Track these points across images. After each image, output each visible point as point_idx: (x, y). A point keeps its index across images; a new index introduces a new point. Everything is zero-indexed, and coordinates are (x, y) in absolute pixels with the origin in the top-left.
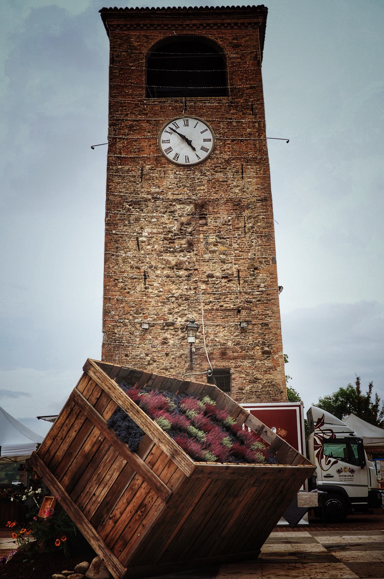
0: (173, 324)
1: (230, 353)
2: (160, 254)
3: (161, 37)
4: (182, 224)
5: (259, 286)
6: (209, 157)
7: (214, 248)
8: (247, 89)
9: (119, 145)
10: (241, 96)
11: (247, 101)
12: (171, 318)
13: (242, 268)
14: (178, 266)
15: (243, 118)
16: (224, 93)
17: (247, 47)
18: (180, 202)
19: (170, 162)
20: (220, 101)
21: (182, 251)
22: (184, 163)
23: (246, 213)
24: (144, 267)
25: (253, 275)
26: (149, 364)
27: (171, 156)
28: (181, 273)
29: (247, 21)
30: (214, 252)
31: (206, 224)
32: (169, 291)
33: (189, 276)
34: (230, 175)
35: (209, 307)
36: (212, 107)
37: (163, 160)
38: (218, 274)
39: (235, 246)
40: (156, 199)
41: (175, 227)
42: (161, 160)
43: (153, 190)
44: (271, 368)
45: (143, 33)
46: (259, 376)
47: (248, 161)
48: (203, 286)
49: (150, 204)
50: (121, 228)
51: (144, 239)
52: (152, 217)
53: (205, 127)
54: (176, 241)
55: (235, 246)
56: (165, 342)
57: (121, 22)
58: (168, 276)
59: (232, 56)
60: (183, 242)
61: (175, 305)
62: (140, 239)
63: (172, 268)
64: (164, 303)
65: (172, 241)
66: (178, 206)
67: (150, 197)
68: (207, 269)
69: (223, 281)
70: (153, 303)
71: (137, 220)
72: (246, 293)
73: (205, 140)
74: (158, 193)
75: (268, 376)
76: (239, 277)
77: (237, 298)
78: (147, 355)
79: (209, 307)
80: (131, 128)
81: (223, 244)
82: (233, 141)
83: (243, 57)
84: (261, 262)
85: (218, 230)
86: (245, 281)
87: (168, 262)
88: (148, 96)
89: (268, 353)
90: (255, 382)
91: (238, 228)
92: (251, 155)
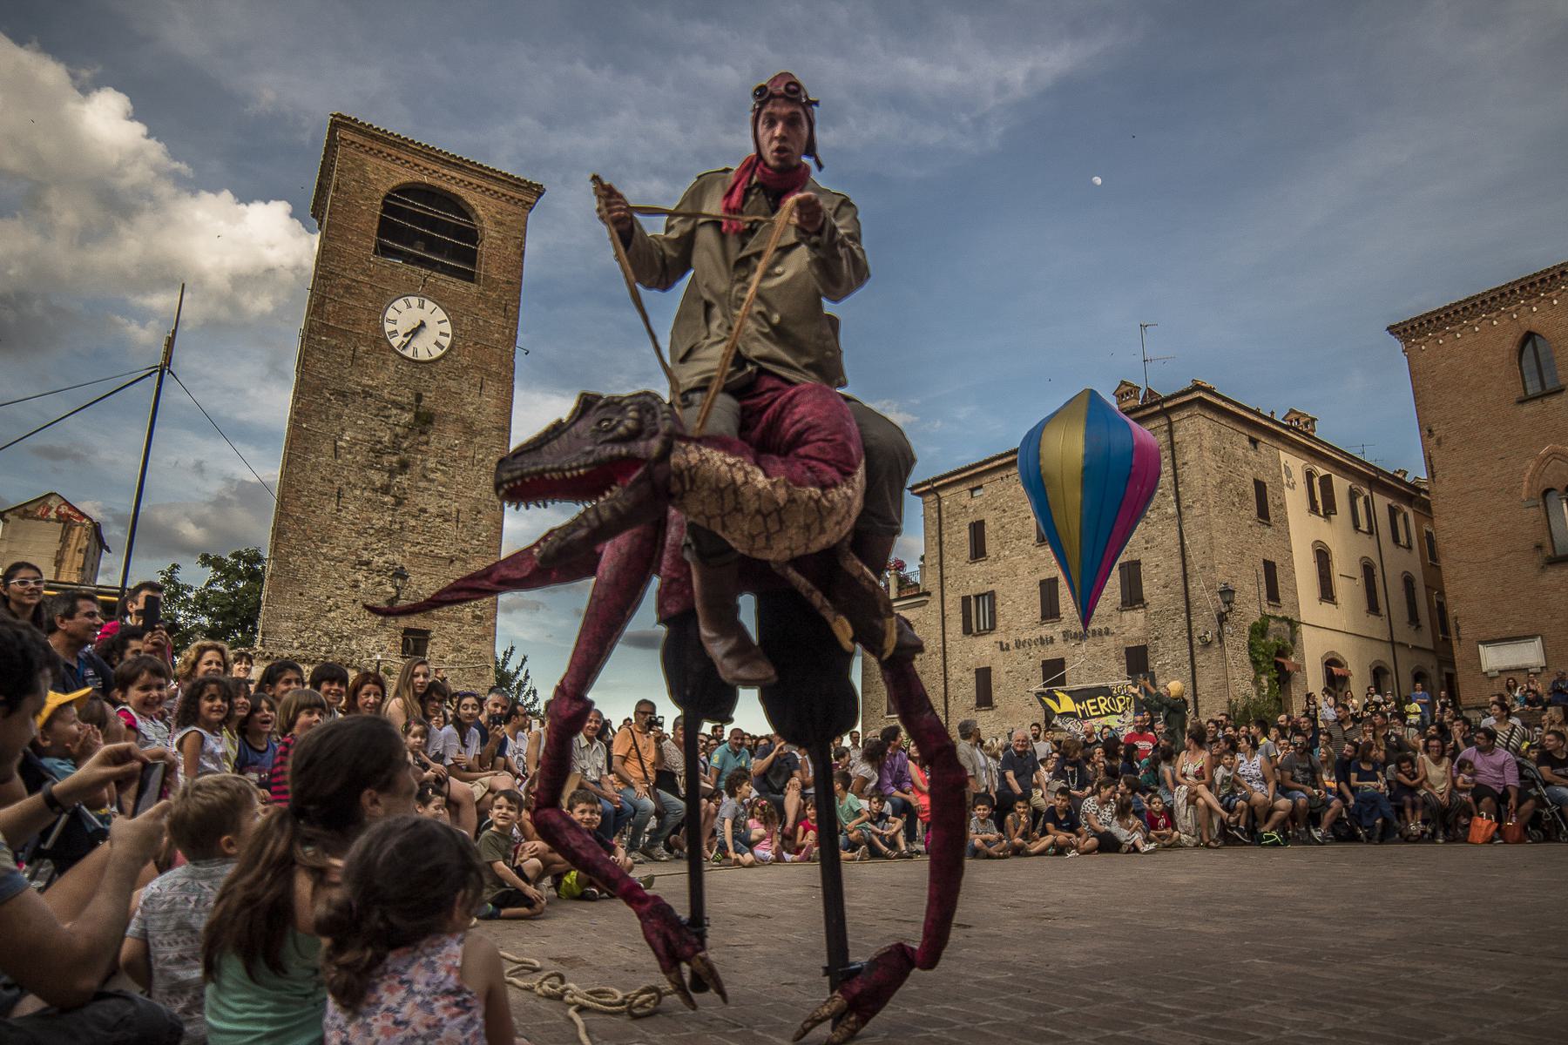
0: (368, 563)
2: (362, 468)
3: (407, 179)
4: (396, 436)
6: (442, 357)
7: (432, 476)
10: (494, 290)
12: (366, 556)
17: (513, 228)
18: (395, 404)
19: (392, 349)
23: (478, 440)
29: (517, 196)
31: (427, 443)
32: (369, 520)
34: (465, 386)
35: (416, 549)
37: (385, 345)
39: (459, 479)
40: (367, 394)
43: (366, 381)
45: (384, 163)
48: (413, 522)
52: (359, 418)
55: (459, 479)
56: (355, 585)
57: (359, 139)
58: (369, 500)
59: (493, 234)
60: (395, 459)
61: (374, 539)
65: (379, 454)
66: (394, 411)
68: (420, 500)
70: (345, 531)
71: (339, 416)
79: (416, 549)
80: (347, 288)
85: (440, 456)
88: (376, 252)
89: (480, 618)
92: (494, 367)
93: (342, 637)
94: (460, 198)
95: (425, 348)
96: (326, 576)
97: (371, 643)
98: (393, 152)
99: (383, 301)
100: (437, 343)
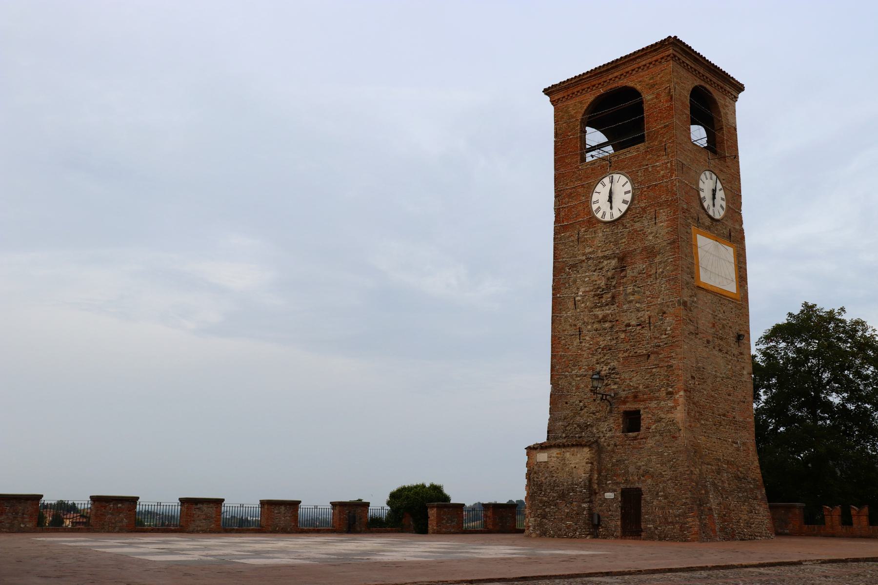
1: (640, 396)
4: (608, 279)
5: (666, 330)
7: (632, 298)
8: (661, 128)
9: (562, 214)
11: (661, 142)
12: (598, 368)
13: (653, 314)
14: (604, 320)
15: (657, 161)
16: (641, 139)
17: (662, 84)
19: (599, 221)
20: (638, 150)
21: (607, 305)
22: (609, 220)
23: (658, 259)
24: (579, 324)
25: (661, 320)
26: (581, 410)
27: (599, 215)
28: (607, 325)
30: (631, 302)
31: (625, 276)
32: (597, 343)
33: (611, 328)
35: (626, 354)
36: (631, 158)
38: (633, 323)
39: (648, 293)
40: (588, 259)
41: (602, 283)
42: (592, 221)
43: (588, 250)
44: (672, 407)
45: (578, 99)
46: (663, 416)
47: (660, 205)
48: (623, 336)
49: (584, 264)
50: (564, 291)
51: (579, 298)
52: (585, 277)
53: (626, 180)
54: (604, 296)
55: (648, 293)
61: (601, 356)
62: (577, 299)
63: (599, 322)
64: (593, 354)
65: (600, 296)
66: (606, 262)
67: (584, 258)
69: (639, 328)
71: (575, 282)
72: (655, 338)
73: (626, 193)
74: (590, 253)
75: (670, 415)
76: (650, 323)
77: (648, 343)
78: (580, 402)
79: (626, 354)
81: (638, 292)
82: (648, 187)
83: (658, 96)
84: (668, 306)
86: (655, 327)
87: (596, 316)
90: (659, 421)
91: (650, 275)
92: (664, 198)
93: (587, 426)
94: (626, 87)
95: (620, 208)
96: (578, 388)
97: (604, 427)
98: (579, 88)
99: (590, 190)
100: (625, 202)
